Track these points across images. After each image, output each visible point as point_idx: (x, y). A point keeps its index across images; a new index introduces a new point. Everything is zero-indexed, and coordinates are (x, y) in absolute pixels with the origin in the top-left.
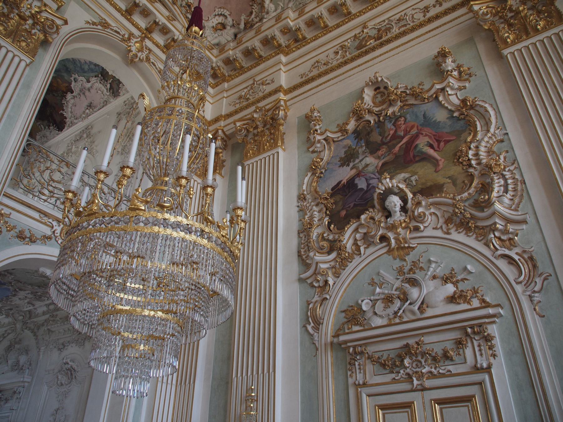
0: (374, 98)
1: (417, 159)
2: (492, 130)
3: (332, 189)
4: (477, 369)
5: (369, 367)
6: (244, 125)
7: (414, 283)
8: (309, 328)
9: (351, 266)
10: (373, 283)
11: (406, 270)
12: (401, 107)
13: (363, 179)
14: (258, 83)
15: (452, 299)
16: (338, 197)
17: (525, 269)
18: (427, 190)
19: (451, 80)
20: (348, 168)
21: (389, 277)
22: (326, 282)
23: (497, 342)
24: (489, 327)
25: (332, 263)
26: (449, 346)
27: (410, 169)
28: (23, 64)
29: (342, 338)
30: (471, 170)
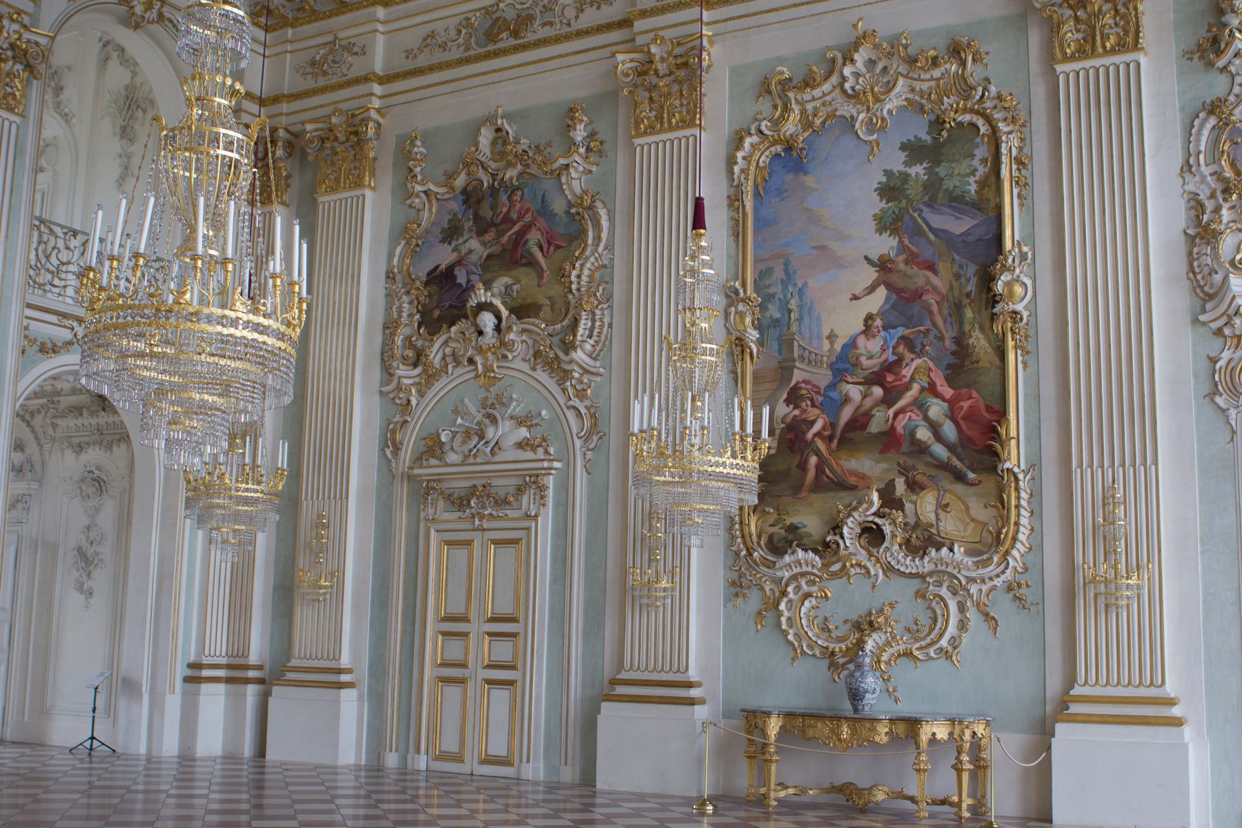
0: (494, 143)
1: (524, 261)
2: (600, 249)
3: (429, 274)
4: (528, 516)
5: (441, 503)
6: (316, 130)
7: (494, 421)
8: (388, 452)
9: (438, 385)
10: (456, 412)
11: (489, 402)
12: (521, 174)
13: (464, 271)
14: (343, 43)
15: (521, 445)
16: (434, 288)
17: (587, 424)
18: (522, 311)
19: (577, 158)
20: (450, 248)
21: (472, 409)
22: (409, 401)
23: (550, 493)
24: (545, 478)
25: (417, 380)
26: (512, 490)
27: (514, 273)
28: (14, 127)
29: (416, 472)
30: (570, 296)
